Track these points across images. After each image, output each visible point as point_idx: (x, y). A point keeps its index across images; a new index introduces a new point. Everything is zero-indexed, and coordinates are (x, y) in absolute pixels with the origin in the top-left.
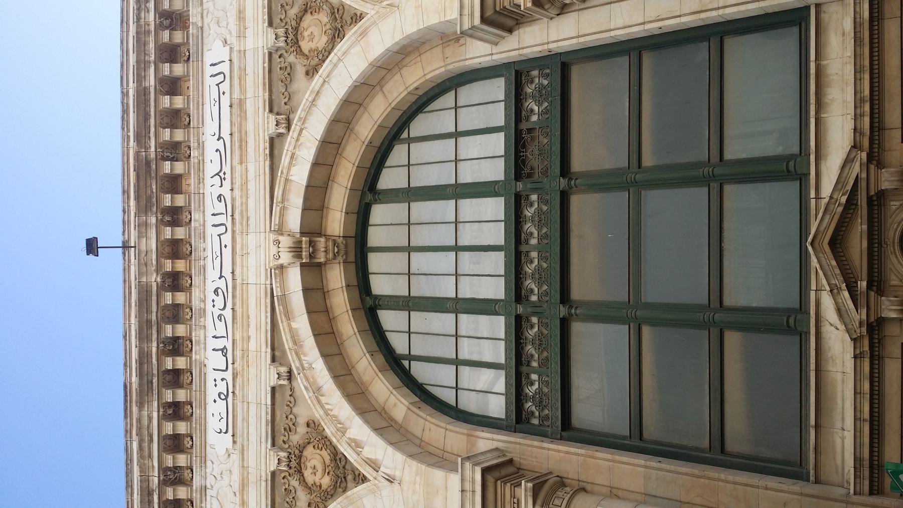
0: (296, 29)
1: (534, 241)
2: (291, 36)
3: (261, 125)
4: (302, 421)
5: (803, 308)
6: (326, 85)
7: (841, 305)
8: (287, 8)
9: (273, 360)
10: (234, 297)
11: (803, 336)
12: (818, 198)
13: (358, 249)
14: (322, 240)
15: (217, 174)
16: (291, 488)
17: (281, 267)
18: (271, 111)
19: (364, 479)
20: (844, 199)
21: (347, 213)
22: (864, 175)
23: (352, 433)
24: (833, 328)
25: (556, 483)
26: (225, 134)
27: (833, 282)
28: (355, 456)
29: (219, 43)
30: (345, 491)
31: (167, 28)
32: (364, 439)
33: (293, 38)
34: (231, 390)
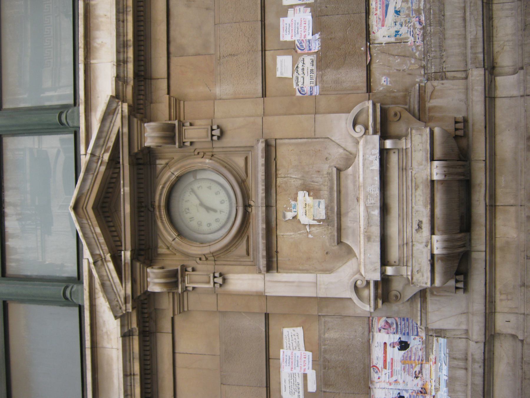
7: (106, 278)
11: (81, 309)
20: (106, 157)
22: (126, 130)
27: (98, 252)
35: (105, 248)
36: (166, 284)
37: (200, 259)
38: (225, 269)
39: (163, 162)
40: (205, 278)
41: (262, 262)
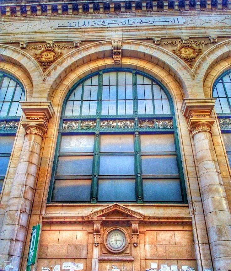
0: (188, 47)
1: (119, 124)
2: (186, 45)
3: (157, 34)
4: (62, 51)
5: (98, 201)
6: (170, 57)
8: (196, 43)
9: (82, 41)
10: (102, 28)
11: (89, 202)
12: (130, 206)
13: (118, 69)
14: (120, 57)
15: (142, 21)
16: (41, 48)
17: (111, 43)
18: (162, 39)
19: (44, 72)
20: (129, 213)
21: (129, 65)
22: (136, 219)
23: (58, 67)
24: (92, 210)
25: (44, 130)
26: (155, 24)
28: (51, 69)
29: (184, 21)
30: (41, 65)
31: (190, 3)
32: (57, 71)
33: (186, 47)
34: (72, 28)
35: (106, 213)
36: (96, 230)
37: (102, 239)
38: (99, 247)
39: (128, 229)
40: (97, 241)
41: (101, 258)
